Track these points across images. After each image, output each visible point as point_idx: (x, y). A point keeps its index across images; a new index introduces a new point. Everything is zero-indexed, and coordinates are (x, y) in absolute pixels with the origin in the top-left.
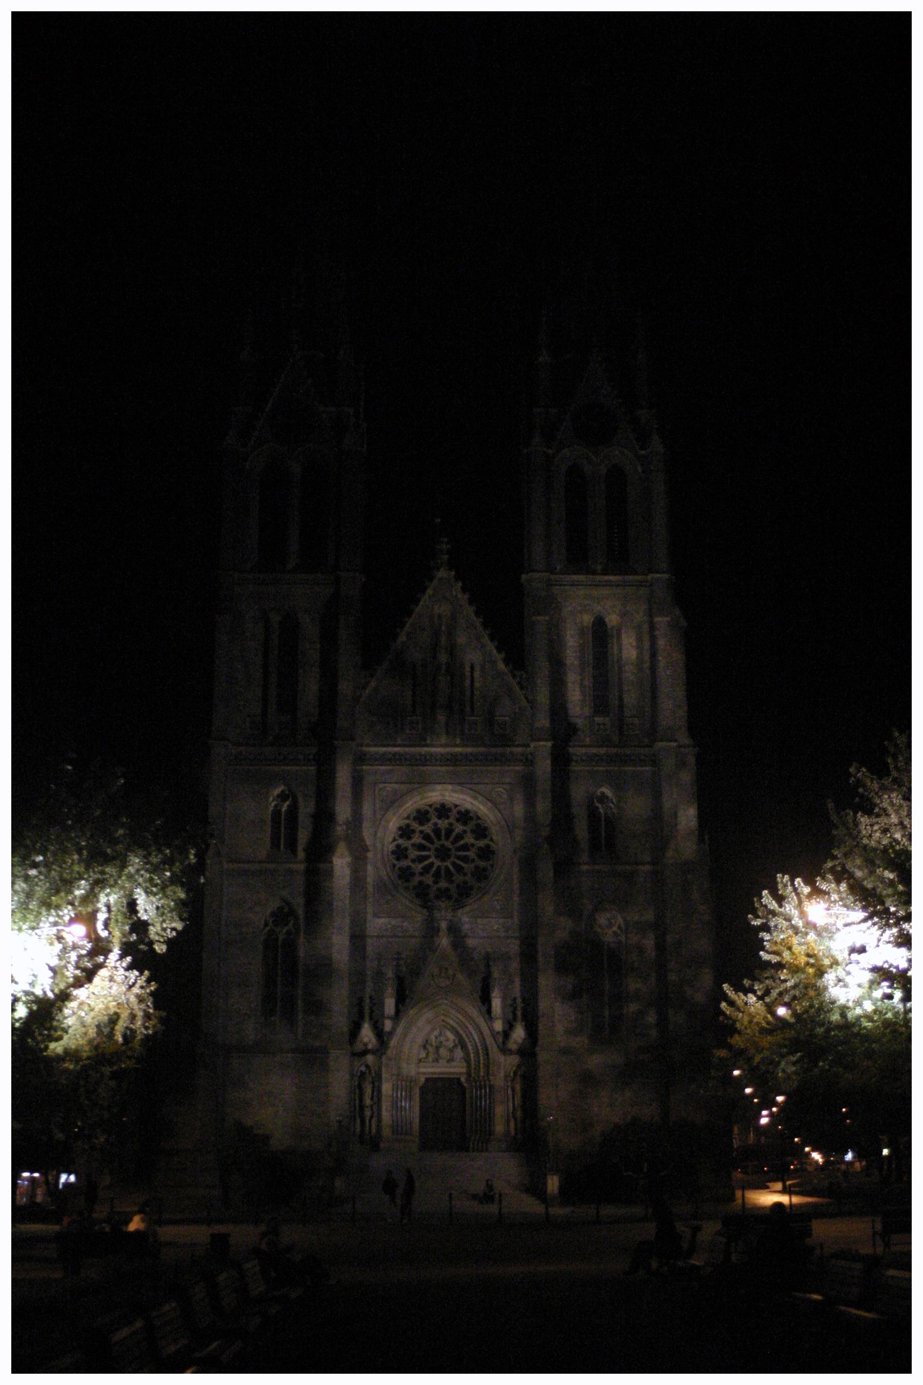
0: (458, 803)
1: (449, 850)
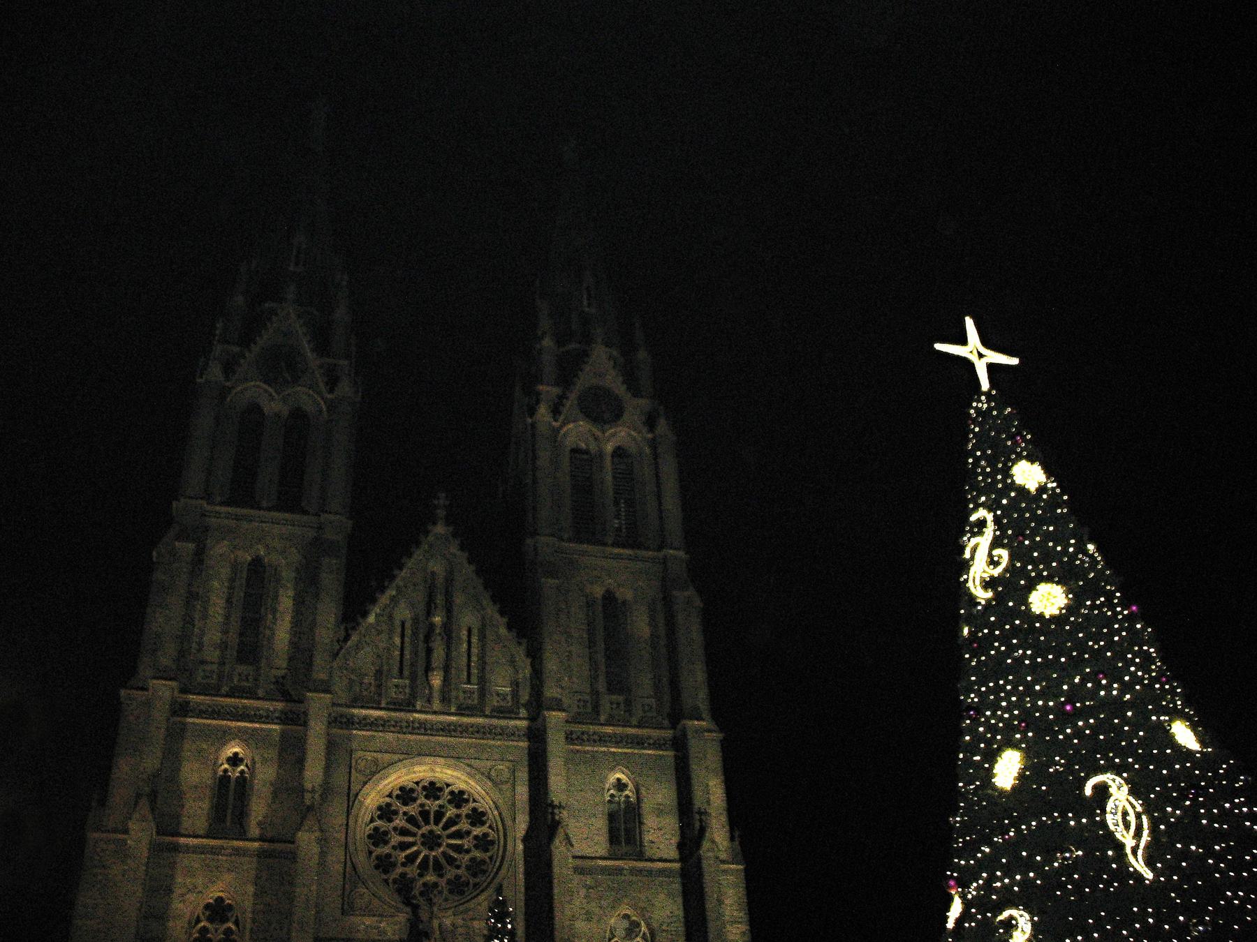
0: (450, 781)
1: (439, 837)
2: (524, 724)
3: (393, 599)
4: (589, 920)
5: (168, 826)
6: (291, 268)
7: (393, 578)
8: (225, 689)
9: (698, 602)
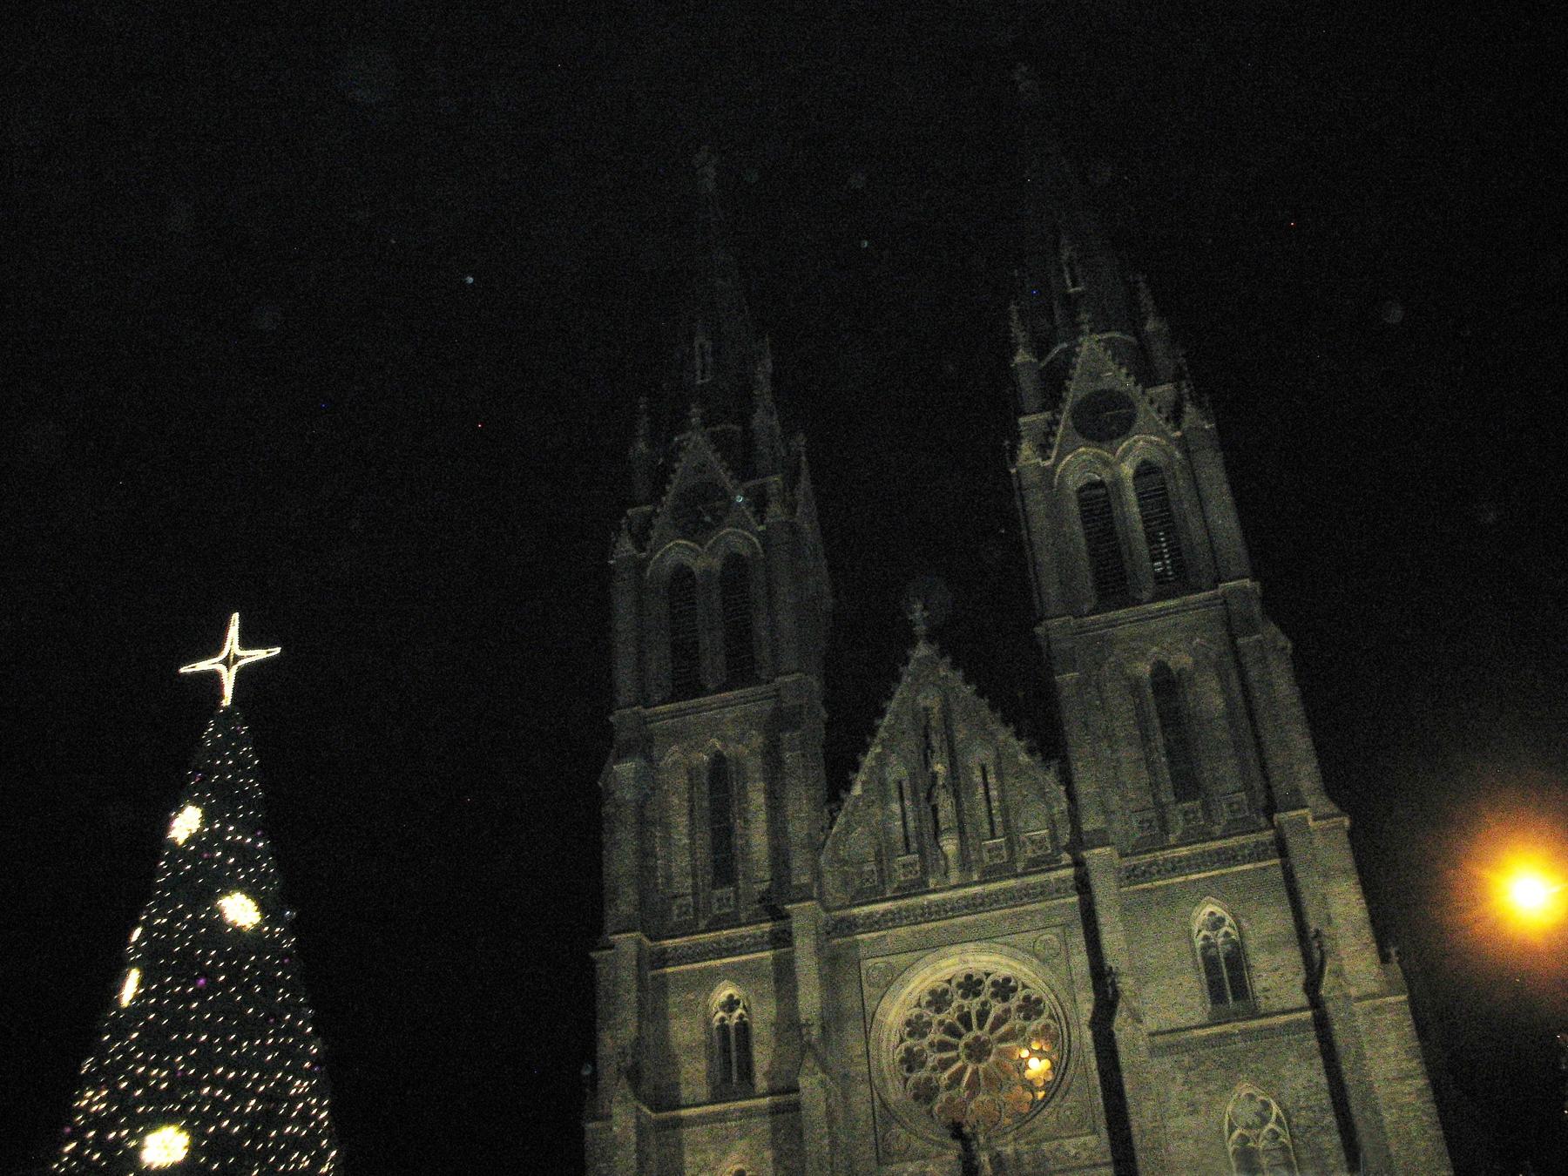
0: (989, 970)
2: (1070, 872)
3: (878, 757)
4: (1194, 1112)
5: (665, 1098)
6: (699, 382)
7: (873, 732)
8: (702, 924)
9: (1283, 641)
